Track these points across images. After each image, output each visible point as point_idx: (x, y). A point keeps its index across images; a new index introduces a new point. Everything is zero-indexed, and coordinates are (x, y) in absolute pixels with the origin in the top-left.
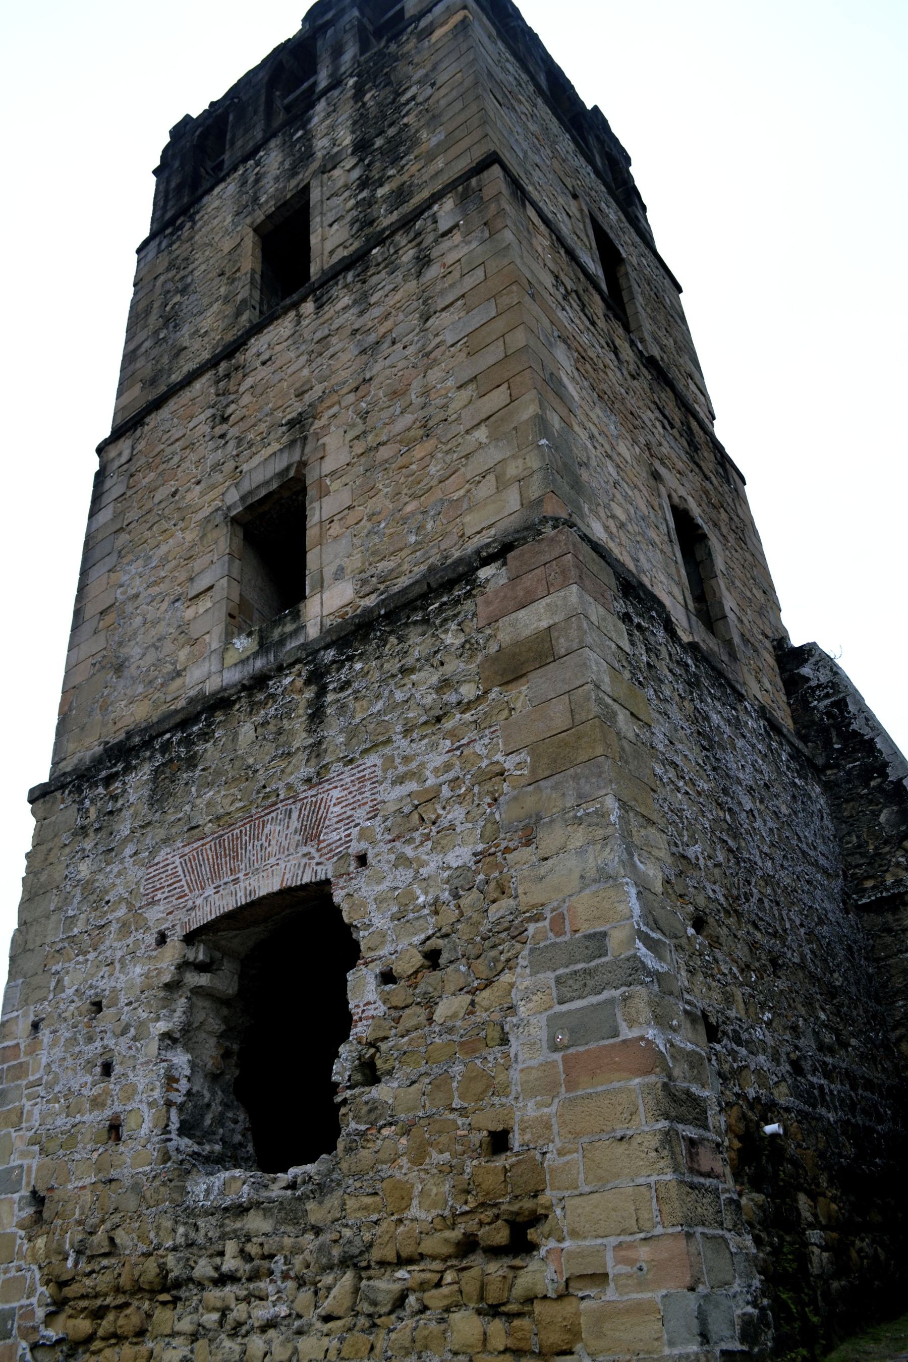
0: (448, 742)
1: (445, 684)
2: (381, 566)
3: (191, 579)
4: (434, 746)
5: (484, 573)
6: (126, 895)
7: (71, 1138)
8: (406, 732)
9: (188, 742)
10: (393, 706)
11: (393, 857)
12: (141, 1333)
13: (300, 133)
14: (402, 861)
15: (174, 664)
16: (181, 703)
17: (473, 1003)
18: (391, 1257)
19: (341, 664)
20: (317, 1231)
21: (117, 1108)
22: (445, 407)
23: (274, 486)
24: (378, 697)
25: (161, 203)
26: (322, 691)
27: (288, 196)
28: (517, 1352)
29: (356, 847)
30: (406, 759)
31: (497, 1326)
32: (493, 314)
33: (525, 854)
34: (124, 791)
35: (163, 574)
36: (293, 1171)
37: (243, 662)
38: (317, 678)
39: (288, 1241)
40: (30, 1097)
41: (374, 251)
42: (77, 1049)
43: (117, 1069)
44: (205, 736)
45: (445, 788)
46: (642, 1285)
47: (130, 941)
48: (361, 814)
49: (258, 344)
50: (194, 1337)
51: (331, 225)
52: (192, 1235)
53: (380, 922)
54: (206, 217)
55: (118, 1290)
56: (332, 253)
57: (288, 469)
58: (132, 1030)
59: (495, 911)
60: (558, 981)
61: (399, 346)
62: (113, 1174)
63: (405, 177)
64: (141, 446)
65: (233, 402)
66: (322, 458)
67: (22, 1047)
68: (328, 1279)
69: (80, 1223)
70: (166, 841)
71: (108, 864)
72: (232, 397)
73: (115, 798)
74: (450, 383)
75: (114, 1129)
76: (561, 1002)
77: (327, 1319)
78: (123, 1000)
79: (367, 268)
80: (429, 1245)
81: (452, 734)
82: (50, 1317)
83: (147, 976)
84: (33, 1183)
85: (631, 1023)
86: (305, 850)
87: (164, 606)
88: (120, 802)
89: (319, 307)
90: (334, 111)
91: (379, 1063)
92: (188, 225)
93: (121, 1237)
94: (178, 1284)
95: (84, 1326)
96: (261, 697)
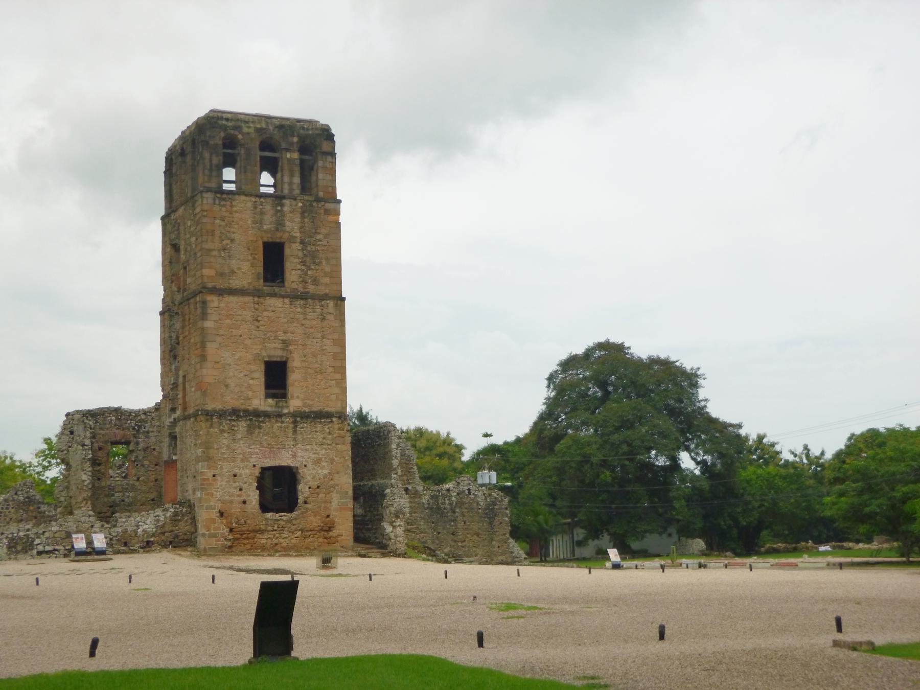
0: (324, 450)
1: (324, 438)
2: (308, 402)
3: (252, 372)
4: (321, 450)
5: (334, 419)
6: (242, 453)
7: (231, 502)
8: (316, 444)
9: (259, 422)
10: (313, 438)
11: (312, 467)
12: (254, 538)
13: (279, 208)
14: (314, 469)
15: (248, 395)
16: (251, 408)
17: (325, 496)
18: (309, 529)
19: (301, 423)
20: (294, 525)
21: (245, 498)
22: (326, 369)
23: (279, 359)
24: (310, 434)
25: (208, 167)
26: (296, 426)
27: (278, 240)
28: (328, 543)
29: (305, 463)
30: (316, 450)
31: (325, 540)
32: (340, 351)
33: (337, 475)
34: (238, 426)
35: (239, 363)
36: (281, 514)
37: (271, 406)
38: (295, 422)
39: (289, 526)
40: (215, 491)
41: (310, 300)
42: (230, 484)
43: (244, 490)
44: (263, 422)
45: (323, 459)
46: (347, 536)
47: (246, 463)
48: (306, 457)
49: (271, 302)
50: (267, 539)
51: (293, 269)
52: (267, 523)
53: (309, 478)
54: (238, 208)
55: (248, 530)
56: (293, 282)
57: (282, 357)
58: (248, 484)
59: (331, 483)
60: (340, 496)
61: (315, 340)
62: (246, 510)
63: (317, 275)
64: (222, 305)
65: (260, 316)
66: (293, 361)
67: (210, 479)
68: (296, 532)
69: (236, 518)
70: (254, 444)
71: (234, 443)
72: (260, 314)
73: (234, 426)
74: (328, 363)
75: (244, 502)
76: (341, 499)
77: (296, 538)
78: (244, 476)
79: (306, 304)
80: (316, 529)
81: (325, 449)
82: (229, 535)
83: (251, 473)
84: (219, 508)
85: (350, 504)
86: (292, 460)
87: (242, 374)
88: (236, 428)
89: (291, 305)
90: (293, 212)
91: (308, 501)
92: (228, 203)
93: (248, 521)
94: (263, 530)
95: (239, 536)
96: (279, 419)
